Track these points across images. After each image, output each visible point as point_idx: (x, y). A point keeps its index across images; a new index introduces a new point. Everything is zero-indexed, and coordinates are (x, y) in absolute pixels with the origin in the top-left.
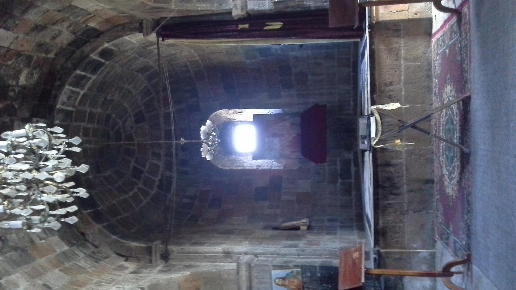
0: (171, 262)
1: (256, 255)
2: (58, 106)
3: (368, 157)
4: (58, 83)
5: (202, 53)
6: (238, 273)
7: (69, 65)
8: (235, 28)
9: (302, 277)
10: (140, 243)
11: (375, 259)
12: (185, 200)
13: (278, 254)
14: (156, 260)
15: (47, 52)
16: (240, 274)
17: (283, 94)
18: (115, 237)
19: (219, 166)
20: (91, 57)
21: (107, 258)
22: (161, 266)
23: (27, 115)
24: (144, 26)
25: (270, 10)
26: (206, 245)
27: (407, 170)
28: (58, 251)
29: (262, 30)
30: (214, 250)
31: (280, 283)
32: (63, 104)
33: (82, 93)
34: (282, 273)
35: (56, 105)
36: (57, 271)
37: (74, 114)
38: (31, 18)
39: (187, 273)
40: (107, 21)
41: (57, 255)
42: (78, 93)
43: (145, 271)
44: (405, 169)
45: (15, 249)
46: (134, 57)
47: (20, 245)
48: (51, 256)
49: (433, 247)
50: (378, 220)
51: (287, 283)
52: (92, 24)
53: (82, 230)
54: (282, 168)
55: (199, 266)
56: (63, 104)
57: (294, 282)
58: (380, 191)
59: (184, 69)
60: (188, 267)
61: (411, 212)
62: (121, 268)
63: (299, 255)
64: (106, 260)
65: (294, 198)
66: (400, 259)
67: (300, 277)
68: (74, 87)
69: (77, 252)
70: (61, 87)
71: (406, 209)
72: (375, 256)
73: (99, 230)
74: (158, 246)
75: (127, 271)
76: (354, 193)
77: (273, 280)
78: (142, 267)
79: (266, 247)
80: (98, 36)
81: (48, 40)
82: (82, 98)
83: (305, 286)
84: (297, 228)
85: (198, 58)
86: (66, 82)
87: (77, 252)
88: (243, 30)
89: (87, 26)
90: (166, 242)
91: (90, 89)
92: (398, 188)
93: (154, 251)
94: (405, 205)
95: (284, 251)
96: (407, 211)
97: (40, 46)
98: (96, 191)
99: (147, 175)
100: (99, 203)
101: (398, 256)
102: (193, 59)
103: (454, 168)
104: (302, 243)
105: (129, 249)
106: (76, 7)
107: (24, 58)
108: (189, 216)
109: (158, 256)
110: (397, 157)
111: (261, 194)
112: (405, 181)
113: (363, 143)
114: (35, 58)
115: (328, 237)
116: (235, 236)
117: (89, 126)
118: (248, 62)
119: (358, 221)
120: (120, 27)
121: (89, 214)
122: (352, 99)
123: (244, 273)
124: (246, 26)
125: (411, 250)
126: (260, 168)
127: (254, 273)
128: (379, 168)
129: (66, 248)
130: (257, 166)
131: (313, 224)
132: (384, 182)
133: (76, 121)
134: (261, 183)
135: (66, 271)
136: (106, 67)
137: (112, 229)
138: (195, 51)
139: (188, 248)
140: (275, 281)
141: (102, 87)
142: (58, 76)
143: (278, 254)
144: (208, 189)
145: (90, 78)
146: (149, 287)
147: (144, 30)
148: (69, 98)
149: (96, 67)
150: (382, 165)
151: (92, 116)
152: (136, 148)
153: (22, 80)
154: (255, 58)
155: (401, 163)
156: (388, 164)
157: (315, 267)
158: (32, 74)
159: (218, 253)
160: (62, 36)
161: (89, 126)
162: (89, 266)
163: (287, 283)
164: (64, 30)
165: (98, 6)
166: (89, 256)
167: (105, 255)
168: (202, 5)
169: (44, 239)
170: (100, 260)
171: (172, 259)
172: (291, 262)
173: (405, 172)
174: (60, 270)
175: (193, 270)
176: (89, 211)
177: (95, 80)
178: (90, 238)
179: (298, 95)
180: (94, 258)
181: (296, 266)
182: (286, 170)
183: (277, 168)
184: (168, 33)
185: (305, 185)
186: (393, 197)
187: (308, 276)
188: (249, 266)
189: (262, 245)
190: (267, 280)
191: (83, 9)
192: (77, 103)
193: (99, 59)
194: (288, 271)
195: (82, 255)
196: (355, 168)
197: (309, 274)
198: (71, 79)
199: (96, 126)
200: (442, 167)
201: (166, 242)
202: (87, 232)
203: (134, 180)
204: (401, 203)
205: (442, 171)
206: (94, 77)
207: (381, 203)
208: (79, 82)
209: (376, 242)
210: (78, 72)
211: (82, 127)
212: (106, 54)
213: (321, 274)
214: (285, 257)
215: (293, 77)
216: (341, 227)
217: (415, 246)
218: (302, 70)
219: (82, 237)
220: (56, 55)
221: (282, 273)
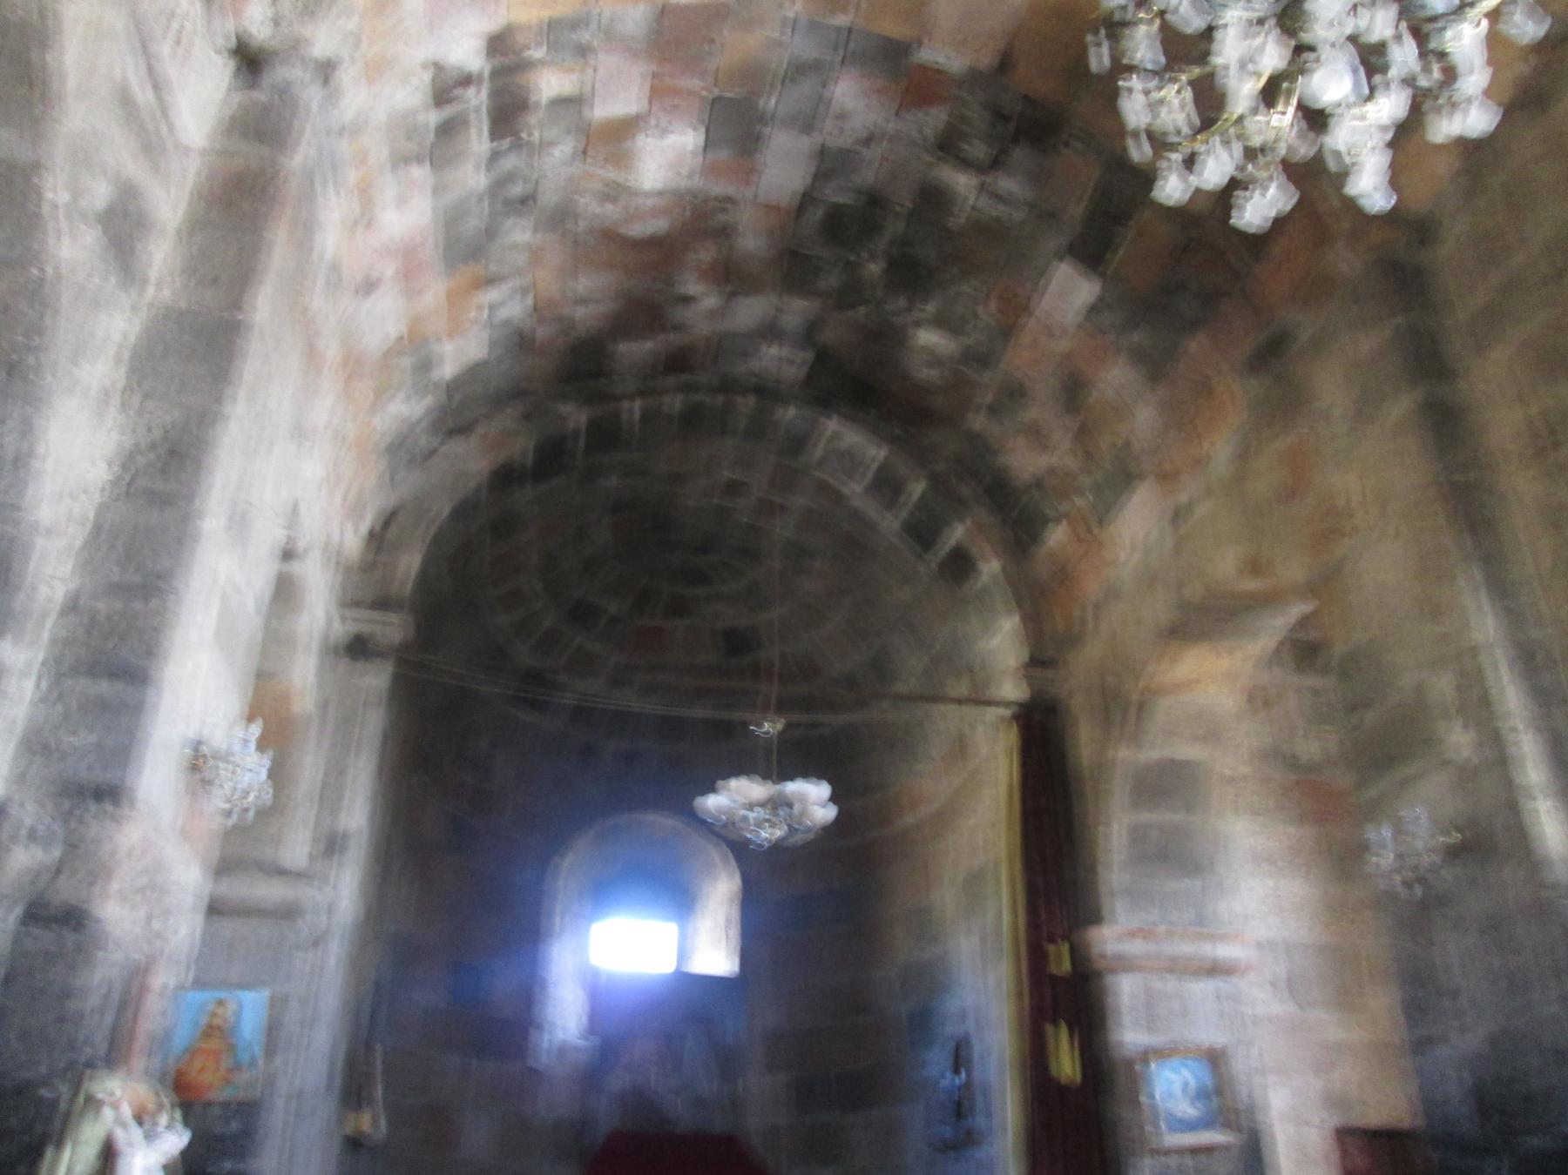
15: (993, 410)
40: (1064, 575)
45: (490, 233)
52: (1057, 537)
74: (393, 629)
109: (366, 629)
141: (854, 545)
149: (923, 532)
153: (929, 338)
188: (288, 913)
208: (887, 485)
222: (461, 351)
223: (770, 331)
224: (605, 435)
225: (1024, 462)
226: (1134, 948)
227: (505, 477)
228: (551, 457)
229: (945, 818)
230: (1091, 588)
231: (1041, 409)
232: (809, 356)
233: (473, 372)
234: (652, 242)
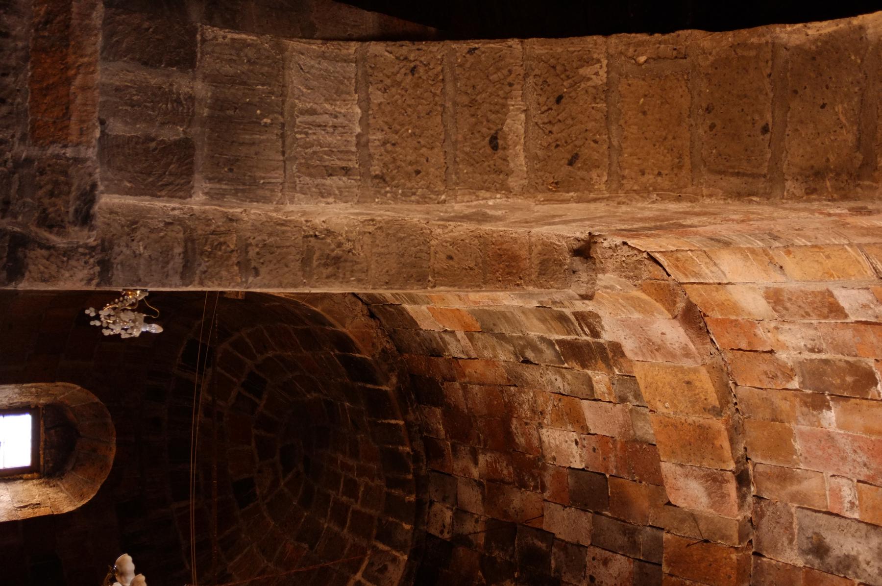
19: (79, 388)
23: (461, 551)
33: (359, 576)
37: (375, 532)
42: (365, 575)
47: (495, 340)
48: (441, 306)
53: (372, 323)
56: (394, 560)
82: (360, 562)
121: (359, 352)
148: (384, 569)
169: (446, 331)
199: (332, 493)
202: (362, 320)
219: (374, 310)
223: (460, 512)
224: (379, 404)
227: (343, 343)
228: (362, 371)
233: (413, 323)
234: (509, 435)
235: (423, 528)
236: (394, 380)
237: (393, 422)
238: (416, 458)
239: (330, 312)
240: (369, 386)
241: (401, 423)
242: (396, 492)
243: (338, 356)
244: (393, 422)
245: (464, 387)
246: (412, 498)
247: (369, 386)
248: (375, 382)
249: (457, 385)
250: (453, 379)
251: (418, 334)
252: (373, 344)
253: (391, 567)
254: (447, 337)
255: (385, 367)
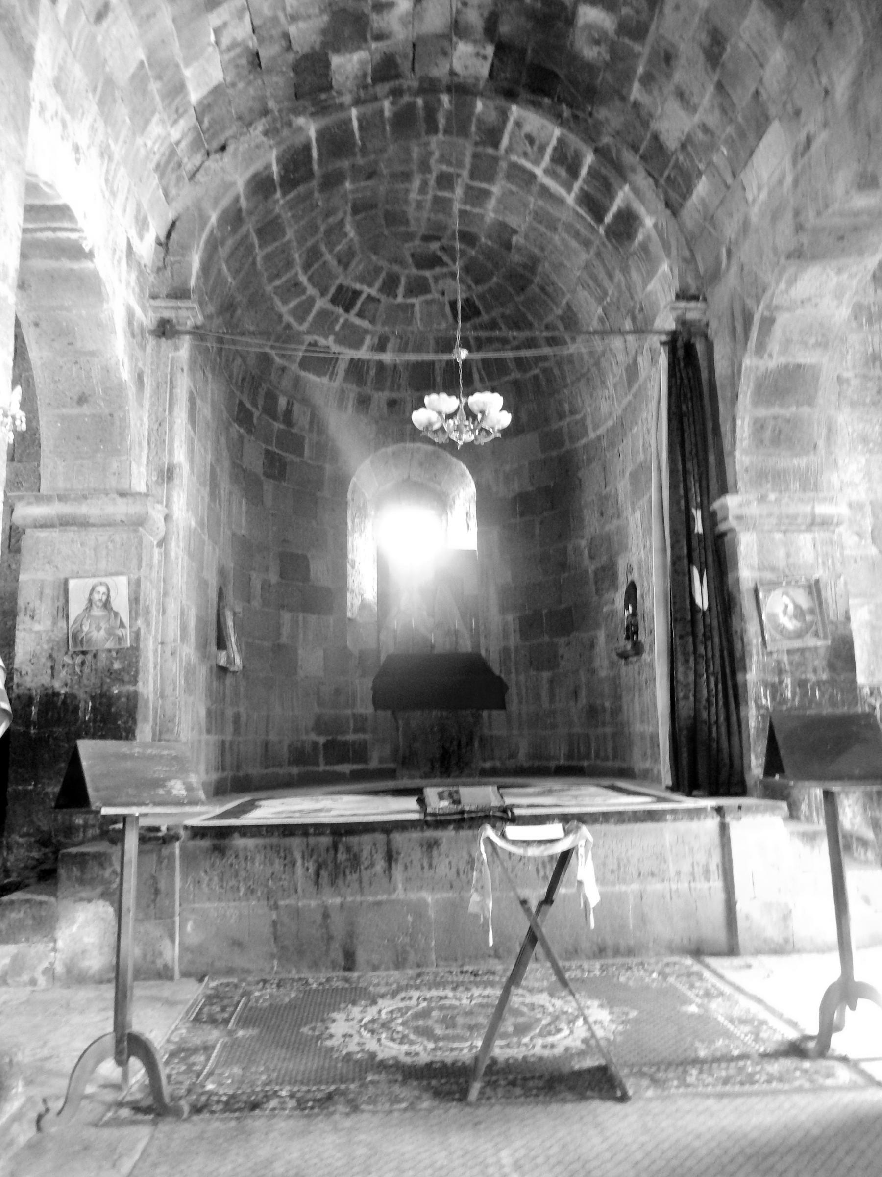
0: (151, 342)
1: (163, 542)
2: (515, 111)
3: (404, 808)
4: (566, 112)
5: (605, 443)
6: (123, 494)
7: (606, 140)
8: (693, 503)
9: (110, 651)
10: (198, 278)
11: (158, 829)
12: (282, 401)
13: (165, 594)
14: (156, 309)
15: (648, 80)
16: (120, 500)
17: (510, 618)
18: (214, 218)
20: (621, 188)
21: (166, 195)
22: (143, 318)
24: (693, 304)
25: (738, 580)
26: (189, 427)
27: (379, 904)
28: (187, 73)
29: (691, 562)
30: (177, 444)
31: (96, 597)
32: (518, 124)
33: (539, 171)
34: (121, 603)
35: (517, 103)
36: (141, 55)
37: (490, 151)
38: (746, 22)
39: (126, 374)
41: (177, 66)
43: (133, 276)
44: (379, 898)
46: (606, 294)
48: (176, 50)
49: (186, 974)
50: (253, 836)
51: (97, 612)
52: (702, 188)
53: (230, 149)
54: (349, 614)
55: (141, 405)
56: (518, 124)
57: (99, 629)
58: (325, 840)
59: (567, 406)
60: (140, 379)
61: (274, 917)
62: (142, 225)
63: (162, 643)
64: (161, 192)
65: (284, 640)
66: (157, 892)
67: (109, 645)
68: (555, 149)
69: (183, 124)
70: (559, 119)
71: (282, 903)
72: (164, 828)
73: (233, 184)
74: (190, 315)
75: (133, 233)
76: (295, 770)
77: (104, 580)
78: (141, 273)
79: (183, 568)
80: (668, 205)
81: (679, 76)
82: (523, 170)
83: (89, 657)
84: (221, 643)
85: (592, 435)
86: (570, 129)
87: (183, 124)
88: (689, 521)
89: (700, 174)
90: (197, 333)
91: (545, 191)
92: (333, 883)
93: (179, 303)
94: (291, 901)
95: (173, 608)
96: (276, 907)
97: (667, 58)
98: (316, 194)
99: (341, 320)
100: (291, 195)
101: (162, 885)
102: (590, 427)
103: (403, 1040)
104: (189, 651)
105: (185, 249)
106: (760, 138)
107: (644, 17)
108: (248, 405)
109: (167, 314)
110: (408, 880)
111: (293, 566)
112: (349, 899)
113: (441, 797)
114: (637, 47)
115: (203, 713)
116: (207, 499)
117: (459, 191)
118: (583, 543)
119: (239, 780)
120: (687, 254)
121: (268, 166)
122: (498, 764)
123: (120, 509)
124: (699, 528)
125: (177, 919)
126: (349, 567)
127: (121, 536)
128: (380, 837)
129: (195, 96)
130: (354, 561)
131: (229, 680)
132: (348, 850)
133: (475, 156)
134: (318, 570)
135: (139, 79)
136: (593, 228)
137: (234, 218)
138: (612, 430)
139: (184, 384)
140: (101, 584)
142: (580, 114)
143: (165, 594)
144: (307, 452)
145: (569, 189)
146: (95, 275)
147: (682, 304)
148: (530, 139)
150: (388, 843)
151: (477, 196)
152: (400, 299)
154: (592, 557)
155: (395, 890)
156: (390, 857)
157: (135, 682)
158: (597, 42)
159: (171, 452)
160: (682, 113)
161: (459, 191)
162: (149, 144)
163: (97, 612)
164: (697, 118)
165: (760, 188)
166: (173, 152)
167: (173, 192)
168: (746, 429)
169: (217, 43)
170: (161, 177)
171: (159, 346)
172: (148, 624)
173: (371, 899)
174: (142, 63)
175: (131, 390)
176: (275, 168)
177: (561, 201)
178: (213, 164)
179: (506, 650)
180: (168, 162)
181: (137, 636)
182: (345, 623)
183: (349, 604)
184: (681, 353)
185: (311, 661)
186: (311, 871)
187: (112, 663)
189: (186, 558)
190: (103, 565)
191: (752, 153)
192: (514, 158)
193: (614, 209)
194: (125, 617)
195: (175, 134)
196: (348, 772)
197: (117, 666)
198: (575, 141)
199: (457, 206)
200: (394, 995)
201: (197, 333)
203: (332, 290)
204: (296, 891)
205: (383, 996)
206: (570, 199)
207: (296, 843)
209: (198, 832)
210: (589, 159)
211: (459, 171)
212: (627, 222)
213: (119, 696)
214: (158, 611)
215: (547, 638)
216: (223, 742)
217: (189, 927)
218: (562, 657)
219: (215, 144)
220: (636, 105)
221: (121, 603)
222: (205, 75)
224: (336, 142)
225: (673, 124)
226: (754, 510)
227: (261, 186)
228: (296, 165)
229: (621, 427)
230: (730, 229)
231: (689, 71)
232: (490, 50)
233: (217, 91)
235: (482, 84)
236: (301, 121)
237: (355, 124)
238: (396, 93)
239: (216, 201)
240: (315, 153)
241: (354, 112)
242: (442, 122)
243: (284, 194)
244: (355, 124)
245: (293, 18)
246: (445, 98)
247: (315, 153)
248: (307, 148)
249: (293, 30)
250: (286, 36)
251: (233, 85)
252: (258, 147)
253: (527, 128)
254: (225, 41)
255: (285, 132)
